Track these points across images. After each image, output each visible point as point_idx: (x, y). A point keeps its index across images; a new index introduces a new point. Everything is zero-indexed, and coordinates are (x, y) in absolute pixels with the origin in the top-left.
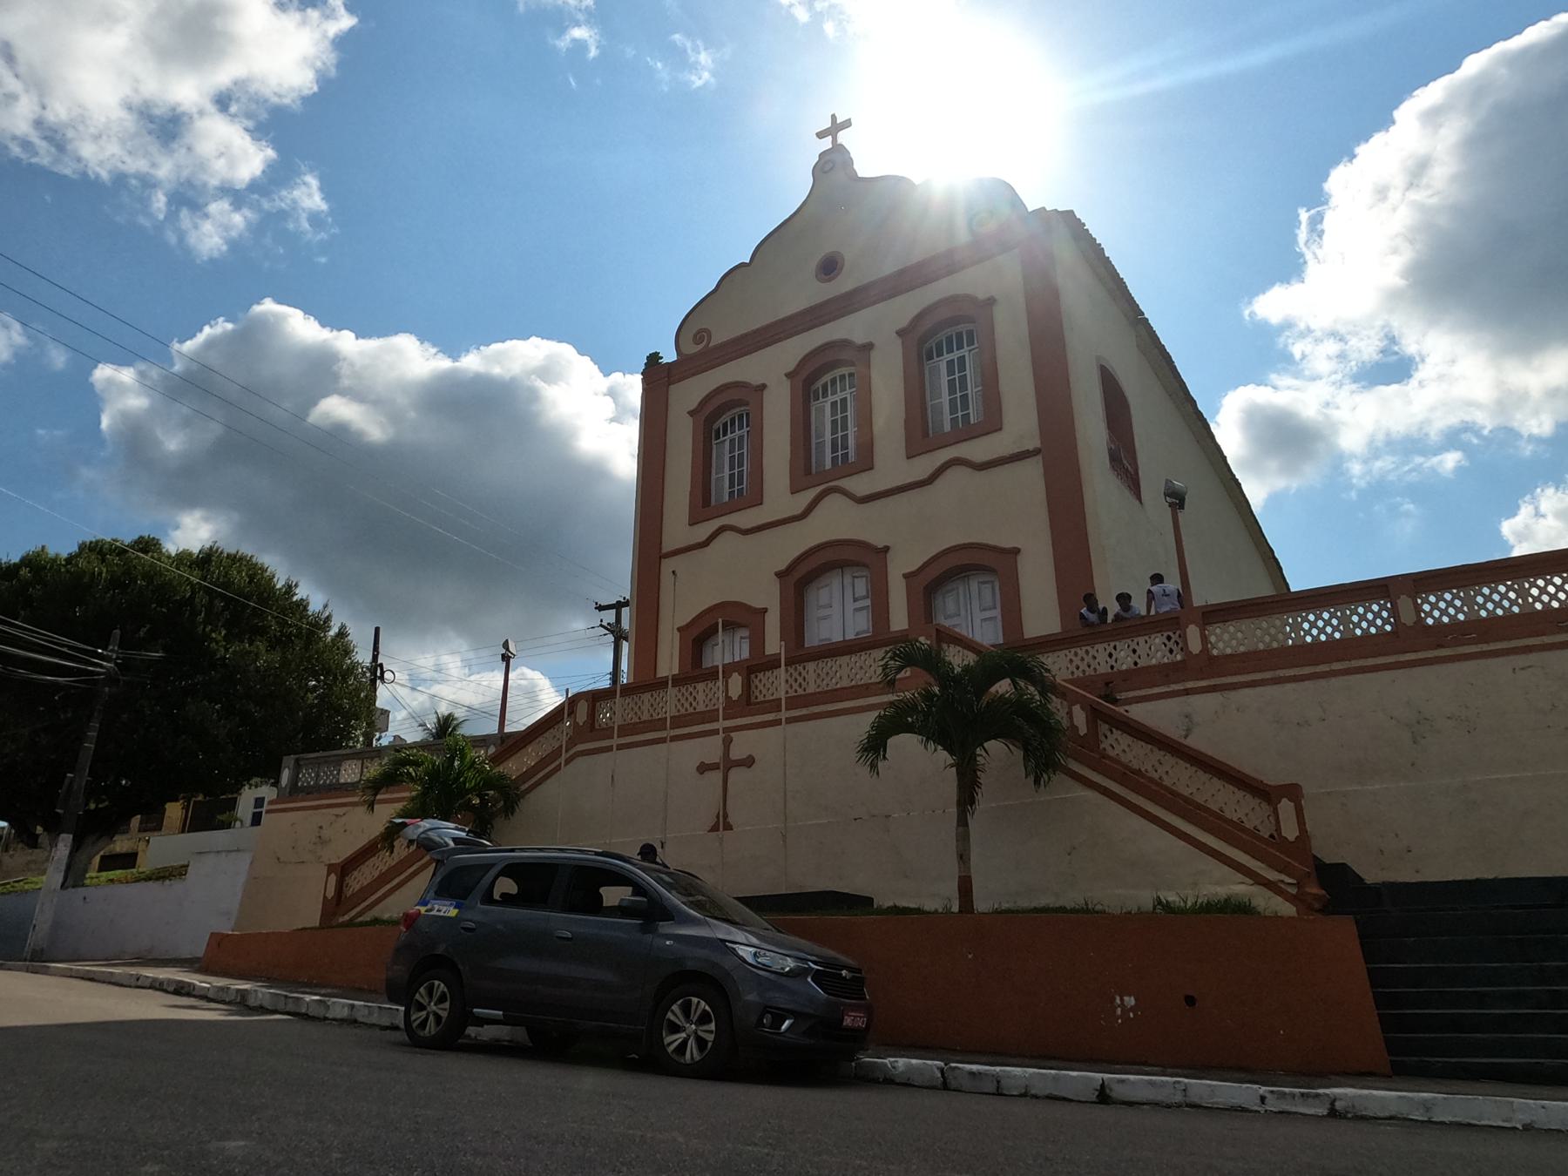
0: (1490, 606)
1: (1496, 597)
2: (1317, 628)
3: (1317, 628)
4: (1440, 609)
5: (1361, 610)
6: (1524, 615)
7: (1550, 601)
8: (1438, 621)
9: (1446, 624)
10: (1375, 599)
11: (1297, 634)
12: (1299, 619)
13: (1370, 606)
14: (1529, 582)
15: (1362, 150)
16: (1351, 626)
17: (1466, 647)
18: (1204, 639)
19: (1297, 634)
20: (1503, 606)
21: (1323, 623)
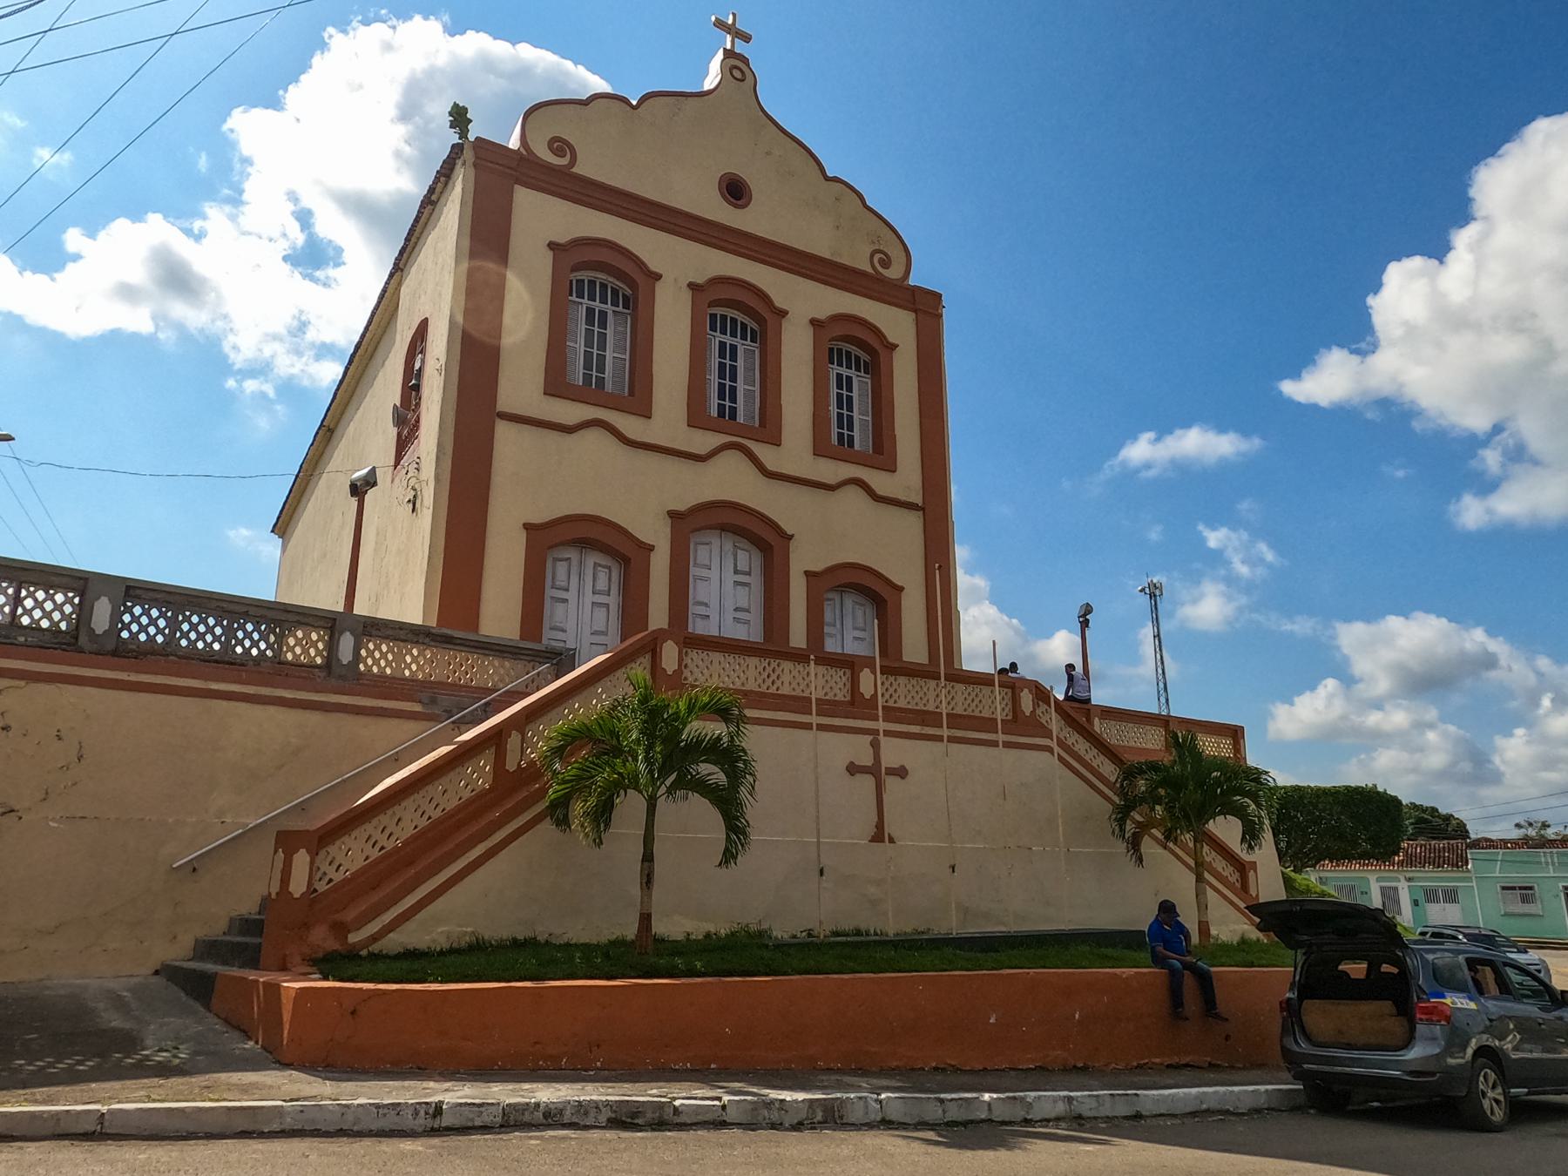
0: (37, 614)
1: (49, 606)
2: (197, 632)
3: (197, 632)
4: (145, 625)
5: (195, 619)
6: (394, 678)
7: (156, 635)
8: (134, 636)
9: (374, 675)
10: (65, 589)
11: (398, 665)
12: (236, 625)
13: (150, 609)
14: (28, 591)
15: (481, 34)
16: (120, 626)
17: (76, 668)
18: (116, 617)
19: (398, 665)
20: (52, 618)
21: (64, 608)
